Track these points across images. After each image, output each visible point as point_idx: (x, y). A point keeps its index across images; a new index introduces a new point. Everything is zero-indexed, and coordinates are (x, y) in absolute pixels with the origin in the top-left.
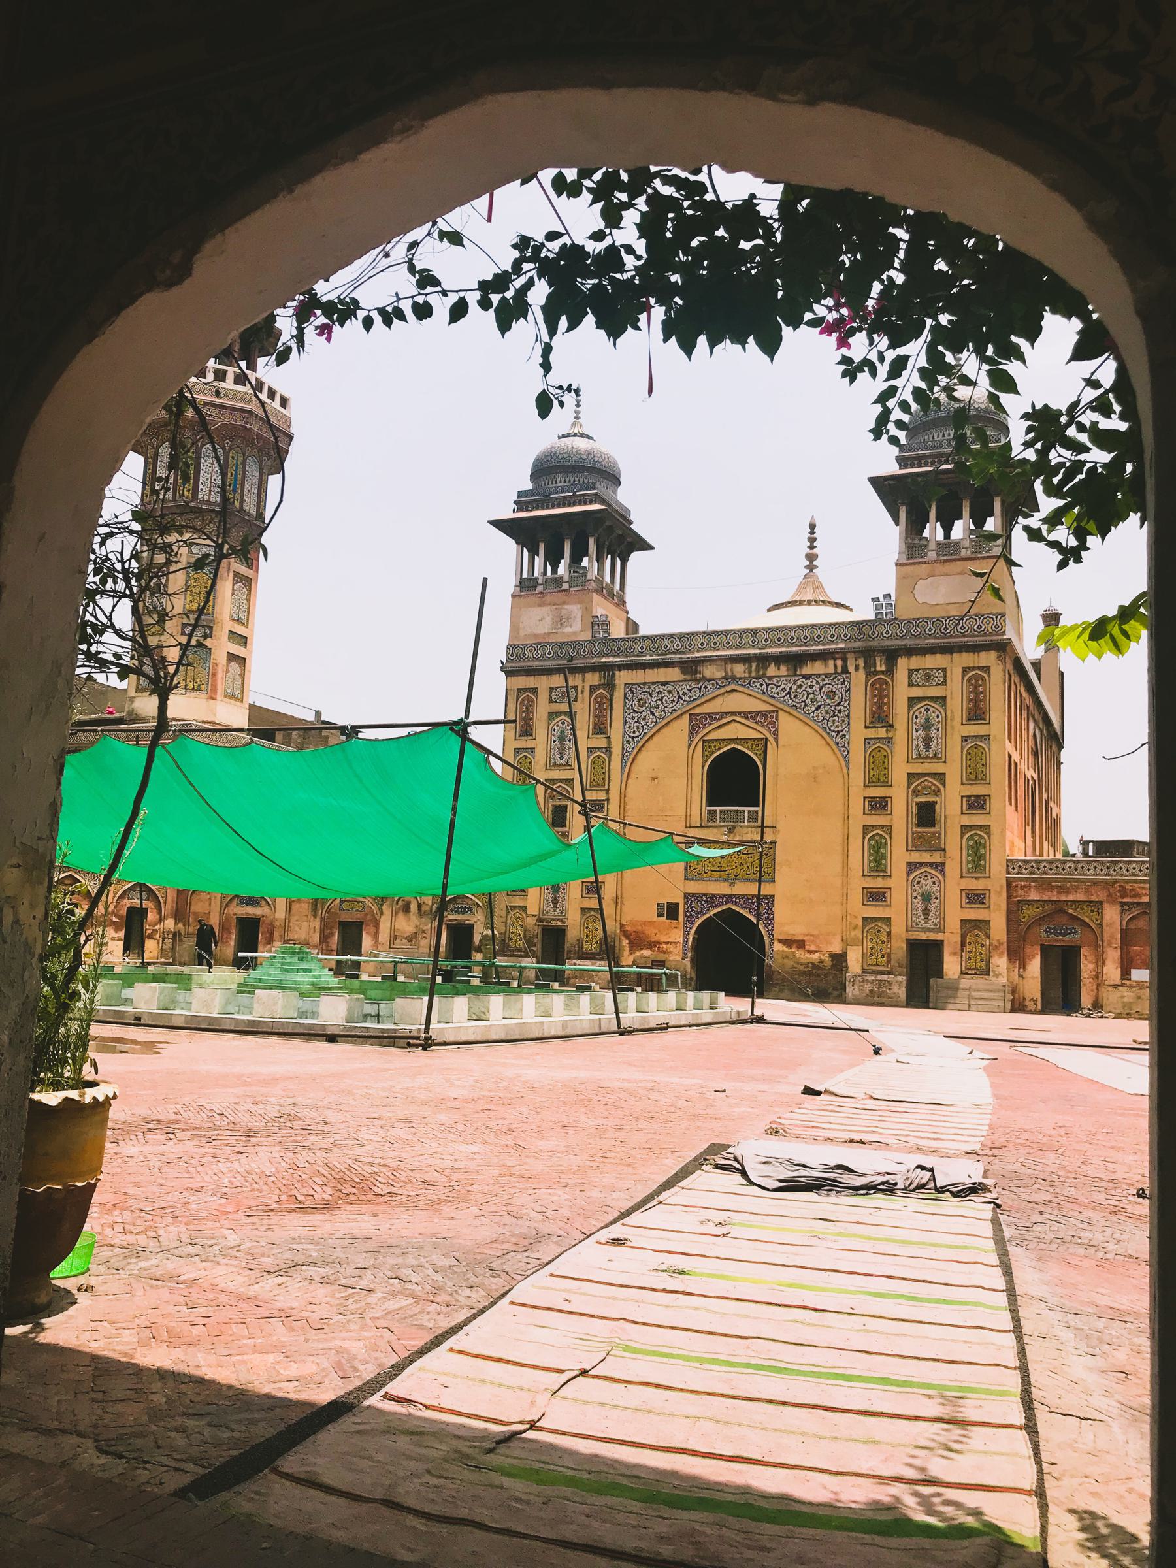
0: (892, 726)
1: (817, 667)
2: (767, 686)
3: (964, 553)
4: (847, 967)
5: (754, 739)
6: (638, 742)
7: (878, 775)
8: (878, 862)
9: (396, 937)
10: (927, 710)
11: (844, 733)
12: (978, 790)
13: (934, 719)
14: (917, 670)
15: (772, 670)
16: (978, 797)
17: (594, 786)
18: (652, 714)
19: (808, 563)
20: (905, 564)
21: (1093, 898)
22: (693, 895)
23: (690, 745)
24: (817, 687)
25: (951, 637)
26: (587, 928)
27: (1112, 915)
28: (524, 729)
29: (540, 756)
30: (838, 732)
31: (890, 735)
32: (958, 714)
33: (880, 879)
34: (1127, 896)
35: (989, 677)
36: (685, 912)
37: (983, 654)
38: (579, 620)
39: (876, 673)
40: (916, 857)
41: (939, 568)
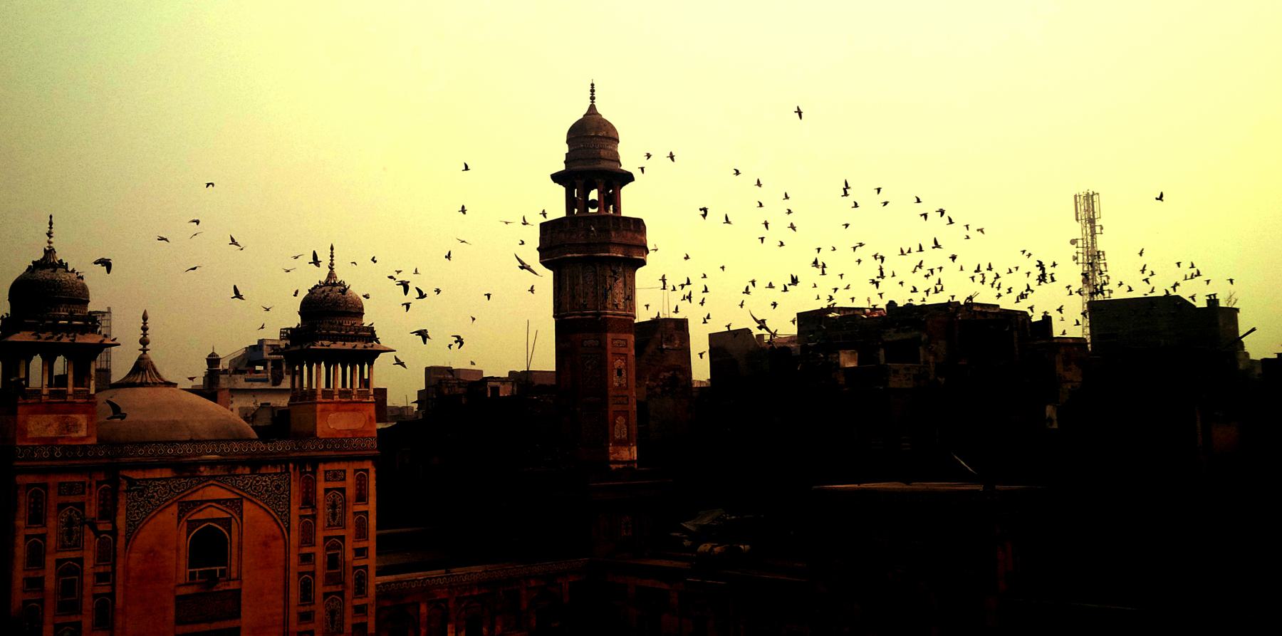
0: (315, 507)
1: (271, 470)
6: (138, 525)
7: (307, 537)
10: (334, 496)
12: (362, 544)
15: (240, 470)
18: (150, 502)
20: (321, 403)
25: (349, 451)
29: (52, 542)
30: (282, 512)
35: (368, 475)
37: (366, 462)
39: (306, 472)
40: (328, 589)
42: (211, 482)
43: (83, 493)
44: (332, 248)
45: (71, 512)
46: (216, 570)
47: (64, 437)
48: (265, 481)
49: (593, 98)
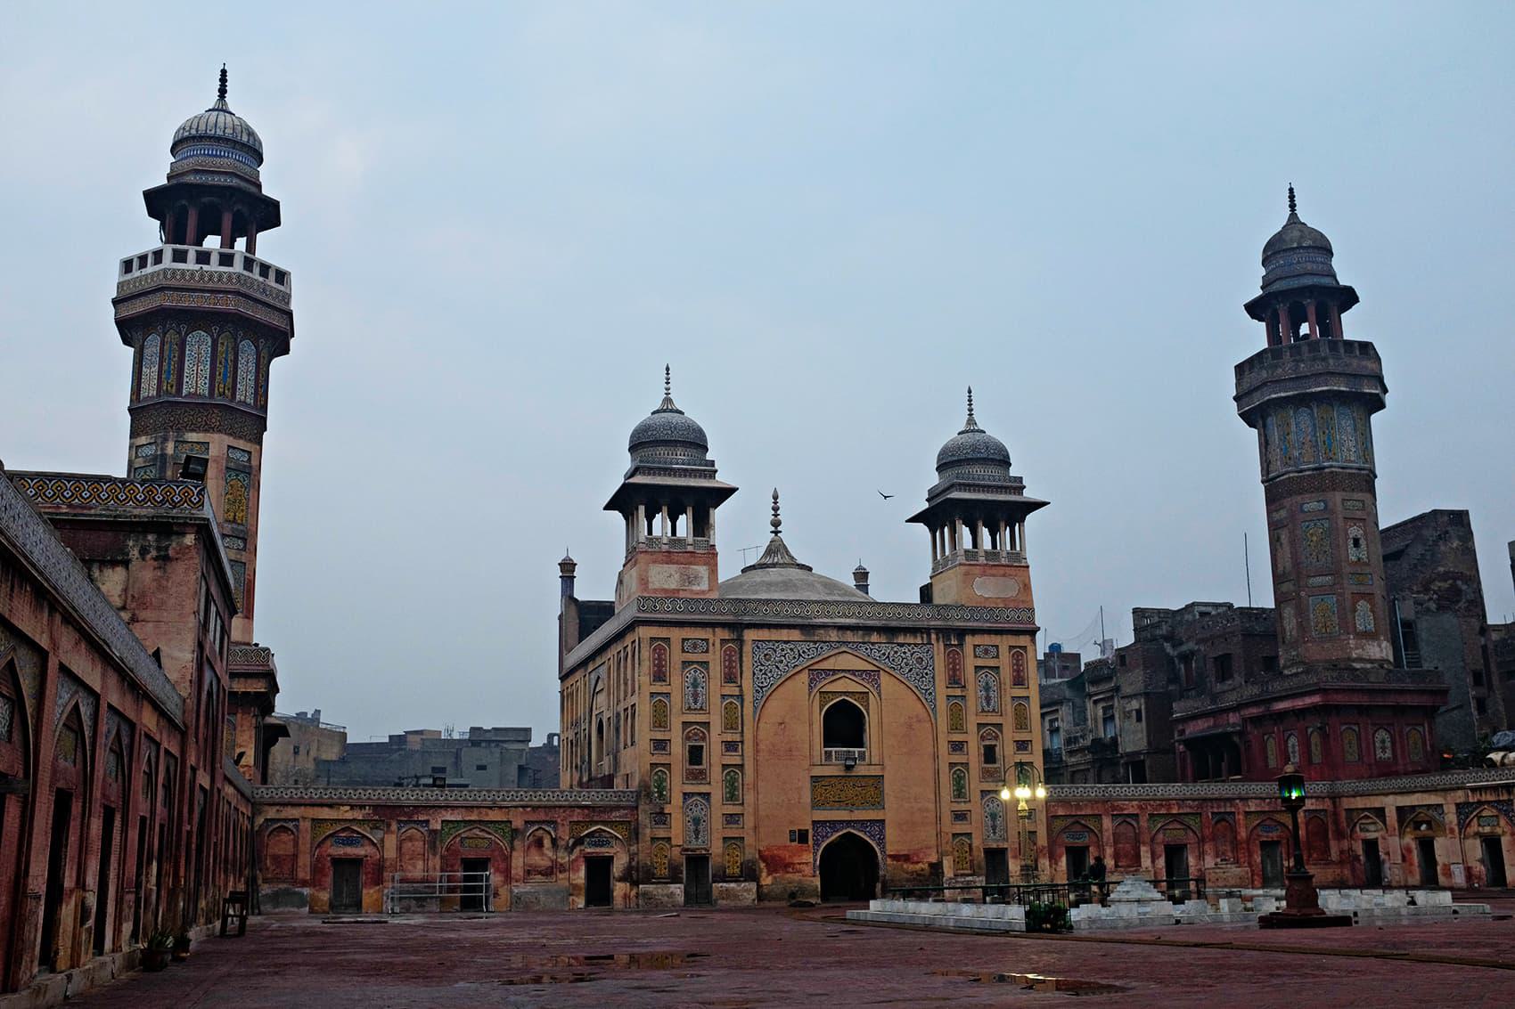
0: (964, 687)
1: (910, 639)
2: (871, 650)
3: (1003, 561)
4: (943, 873)
5: (861, 693)
7: (957, 724)
8: (959, 792)
9: (529, 872)
10: (986, 676)
11: (931, 691)
12: (1023, 736)
13: (991, 684)
14: (979, 646)
15: (875, 638)
16: (1023, 741)
17: (728, 729)
18: (777, 667)
19: (773, 529)
20: (965, 565)
21: (1096, 812)
22: (819, 822)
23: (809, 695)
24: (908, 654)
25: (1000, 623)
26: (728, 855)
27: (1107, 823)
28: (657, 675)
29: (676, 699)
30: (926, 690)
31: (963, 694)
32: (1008, 681)
33: (963, 804)
34: (1116, 810)
36: (814, 836)
38: (706, 579)
41: (989, 571)
42: (844, 649)
43: (707, 651)
44: (970, 392)
45: (695, 672)
46: (854, 752)
47: (686, 590)
48: (905, 653)
49: (1293, 206)
